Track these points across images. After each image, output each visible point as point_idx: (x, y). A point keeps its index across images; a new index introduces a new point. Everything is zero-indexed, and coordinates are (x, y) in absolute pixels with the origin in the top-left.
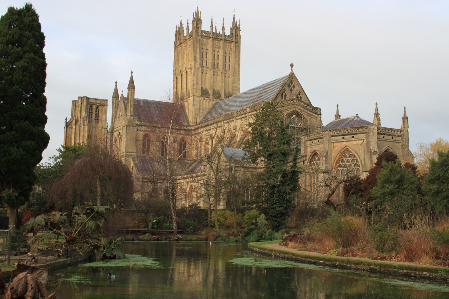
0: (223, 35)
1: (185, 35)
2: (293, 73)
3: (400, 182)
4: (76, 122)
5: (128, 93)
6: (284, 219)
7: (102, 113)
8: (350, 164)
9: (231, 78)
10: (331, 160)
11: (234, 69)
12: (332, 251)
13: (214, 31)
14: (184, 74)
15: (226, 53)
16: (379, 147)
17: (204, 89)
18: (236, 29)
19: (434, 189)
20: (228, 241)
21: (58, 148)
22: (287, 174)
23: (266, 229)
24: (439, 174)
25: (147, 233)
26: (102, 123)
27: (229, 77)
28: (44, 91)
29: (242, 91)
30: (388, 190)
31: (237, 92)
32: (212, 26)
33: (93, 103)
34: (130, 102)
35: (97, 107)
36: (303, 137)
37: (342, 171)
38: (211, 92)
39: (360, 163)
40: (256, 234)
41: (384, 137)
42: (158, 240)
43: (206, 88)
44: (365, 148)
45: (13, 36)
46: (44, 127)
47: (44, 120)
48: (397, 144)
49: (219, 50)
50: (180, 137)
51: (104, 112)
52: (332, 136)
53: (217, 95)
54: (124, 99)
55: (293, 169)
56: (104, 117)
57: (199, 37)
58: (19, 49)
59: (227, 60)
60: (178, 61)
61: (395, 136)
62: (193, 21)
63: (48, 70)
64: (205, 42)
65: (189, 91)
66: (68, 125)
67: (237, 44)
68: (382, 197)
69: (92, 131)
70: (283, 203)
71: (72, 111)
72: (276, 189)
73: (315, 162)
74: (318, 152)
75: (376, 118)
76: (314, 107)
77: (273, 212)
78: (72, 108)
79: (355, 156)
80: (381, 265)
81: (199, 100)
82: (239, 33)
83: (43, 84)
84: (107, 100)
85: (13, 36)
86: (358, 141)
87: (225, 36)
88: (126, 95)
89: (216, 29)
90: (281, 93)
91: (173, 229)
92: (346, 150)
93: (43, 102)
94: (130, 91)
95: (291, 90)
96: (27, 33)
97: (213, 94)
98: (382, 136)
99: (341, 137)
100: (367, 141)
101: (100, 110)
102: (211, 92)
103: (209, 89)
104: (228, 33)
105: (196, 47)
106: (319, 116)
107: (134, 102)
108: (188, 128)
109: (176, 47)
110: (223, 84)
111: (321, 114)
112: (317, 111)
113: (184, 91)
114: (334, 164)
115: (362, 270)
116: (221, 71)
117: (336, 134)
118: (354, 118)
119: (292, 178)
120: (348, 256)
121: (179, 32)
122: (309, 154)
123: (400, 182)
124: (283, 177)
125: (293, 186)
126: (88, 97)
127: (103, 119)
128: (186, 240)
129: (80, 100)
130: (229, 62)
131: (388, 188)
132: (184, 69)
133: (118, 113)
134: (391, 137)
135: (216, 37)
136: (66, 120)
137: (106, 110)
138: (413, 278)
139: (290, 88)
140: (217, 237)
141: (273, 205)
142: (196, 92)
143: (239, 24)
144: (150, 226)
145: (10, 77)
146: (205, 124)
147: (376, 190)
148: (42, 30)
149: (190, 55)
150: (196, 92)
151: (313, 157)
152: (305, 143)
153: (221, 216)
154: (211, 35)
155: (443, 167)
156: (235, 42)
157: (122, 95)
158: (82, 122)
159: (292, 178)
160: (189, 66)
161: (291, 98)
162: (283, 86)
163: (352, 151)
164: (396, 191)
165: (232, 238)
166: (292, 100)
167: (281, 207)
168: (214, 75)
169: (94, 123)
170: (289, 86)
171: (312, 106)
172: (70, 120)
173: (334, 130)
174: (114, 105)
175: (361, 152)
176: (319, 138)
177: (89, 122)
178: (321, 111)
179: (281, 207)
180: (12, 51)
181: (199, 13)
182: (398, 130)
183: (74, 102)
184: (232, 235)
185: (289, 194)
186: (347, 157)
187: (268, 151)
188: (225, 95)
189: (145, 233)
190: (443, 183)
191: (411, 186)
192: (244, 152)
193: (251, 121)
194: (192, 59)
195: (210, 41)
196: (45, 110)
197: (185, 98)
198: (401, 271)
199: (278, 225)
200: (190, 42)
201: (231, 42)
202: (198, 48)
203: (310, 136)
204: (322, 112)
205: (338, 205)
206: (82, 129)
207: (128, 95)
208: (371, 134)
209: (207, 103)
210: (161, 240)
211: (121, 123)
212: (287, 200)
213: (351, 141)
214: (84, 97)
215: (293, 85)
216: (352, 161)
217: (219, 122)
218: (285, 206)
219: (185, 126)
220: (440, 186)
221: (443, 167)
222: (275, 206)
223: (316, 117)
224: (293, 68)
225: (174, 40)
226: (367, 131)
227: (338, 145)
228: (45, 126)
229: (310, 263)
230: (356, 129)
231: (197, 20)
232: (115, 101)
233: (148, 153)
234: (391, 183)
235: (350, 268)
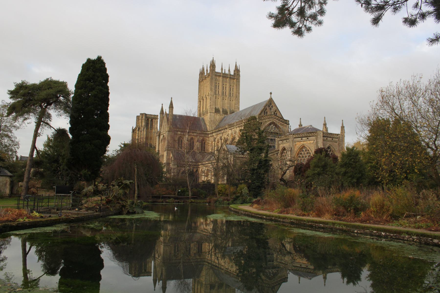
0: (229, 75)
1: (205, 74)
2: (272, 98)
3: (324, 167)
4: (139, 129)
5: (169, 111)
6: (260, 190)
7: (155, 123)
8: (306, 156)
9: (234, 102)
10: (294, 153)
11: (236, 96)
12: (276, 210)
13: (223, 72)
14: (205, 99)
15: (231, 86)
16: (324, 145)
17: (217, 108)
18: (237, 71)
19: (343, 171)
20: (223, 204)
21: (119, 145)
22: (262, 162)
23: (248, 196)
24: (346, 162)
25: (171, 198)
26: (154, 130)
27: (233, 101)
28: (107, 109)
29: (241, 109)
30: (317, 172)
31: (238, 110)
32: (222, 69)
33: (149, 117)
34: (170, 116)
35: (152, 120)
36: (276, 139)
37: (301, 160)
38: (221, 110)
40: (241, 200)
41: (327, 139)
42: (179, 202)
43: (218, 108)
44: (315, 145)
45: (89, 76)
46: (108, 132)
47: (108, 127)
48: (335, 143)
49: (227, 84)
50: (201, 138)
51: (156, 122)
52: (295, 138)
53: (225, 112)
54: (166, 114)
55: (266, 159)
56: (156, 126)
57: (214, 76)
58: (92, 84)
59: (232, 90)
60: (201, 91)
61: (334, 138)
62: (210, 66)
63: (110, 97)
64: (218, 79)
65: (207, 110)
66: (134, 131)
67: (238, 80)
68: (313, 176)
69: (148, 135)
70: (259, 180)
71: (136, 122)
72: (255, 171)
73: (284, 154)
74: (286, 148)
75: (324, 127)
76: (285, 120)
77: (253, 186)
78: (137, 120)
79: (309, 151)
80: (297, 220)
81: (213, 115)
82: (239, 73)
83: (108, 105)
84: (158, 115)
85: (89, 76)
86: (310, 141)
87: (230, 75)
88: (168, 112)
89: (225, 71)
90: (264, 111)
91: (189, 195)
92: (303, 147)
93: (106, 117)
94: (170, 110)
95: (271, 109)
96: (98, 74)
97: (222, 111)
98: (325, 138)
99: (300, 139)
100: (316, 141)
101: (153, 121)
102: (221, 110)
103: (220, 108)
104: (232, 73)
105: (212, 82)
106: (288, 125)
107: (172, 116)
108: (206, 133)
109: (200, 82)
110: (229, 105)
111: (289, 124)
112: (286, 122)
113: (204, 109)
114: (296, 155)
115: (286, 222)
116: (227, 97)
117: (297, 136)
118: (309, 127)
119: (265, 164)
120: (284, 214)
121: (202, 73)
122: (280, 149)
123: (324, 167)
124: (259, 164)
125: (266, 169)
126: (146, 113)
127: (155, 127)
128: (196, 203)
129: (141, 116)
130: (233, 91)
131: (317, 170)
132: (205, 96)
133: (163, 123)
134: (331, 139)
135: (225, 76)
136: (133, 128)
137: (157, 122)
138: (314, 228)
139: (270, 107)
140: (216, 201)
141: (253, 181)
142: (212, 110)
143: (239, 68)
144: (176, 194)
145: (86, 101)
146: (217, 130)
147: (309, 172)
148: (107, 72)
149: (208, 87)
150: (212, 110)
151: (283, 151)
152: (278, 142)
153: (223, 188)
154: (222, 75)
155: (349, 157)
156: (237, 79)
157: (166, 112)
158: (142, 129)
159: (265, 164)
160: (208, 94)
161: (270, 114)
162: (265, 107)
163: (307, 147)
164: (322, 172)
165: (225, 201)
166: (271, 115)
167: (258, 182)
168: (223, 99)
169: (149, 129)
170: (269, 106)
171: (283, 119)
172: (135, 128)
173: (296, 134)
174: (161, 118)
175: (312, 148)
176: (287, 139)
177: (147, 129)
178: (289, 122)
179: (258, 182)
180: (88, 85)
182: (336, 134)
183: (138, 117)
184: (226, 200)
185: (263, 174)
186: (304, 151)
187: (250, 147)
188: (230, 112)
189: (169, 198)
190: (349, 167)
191: (331, 169)
192: (236, 148)
193: (242, 128)
194: (209, 89)
195: (221, 78)
196: (108, 121)
197: (205, 114)
198: (308, 223)
199: (256, 194)
200: (208, 79)
201: (234, 79)
202: (213, 83)
203: (281, 138)
204: (290, 123)
205: (288, 181)
206: (142, 133)
207: (169, 112)
208: (319, 137)
209: (218, 117)
210: (181, 203)
211: (165, 130)
212: (262, 178)
213: (307, 141)
214: (144, 114)
215: (271, 106)
216: (307, 154)
217: (225, 129)
218: (261, 182)
219: (205, 131)
220: (347, 170)
221: (349, 157)
222: (254, 182)
223: (286, 126)
224: (272, 95)
225: (199, 78)
226: (316, 135)
227: (298, 144)
228: (108, 131)
229: (258, 218)
230: (310, 134)
231: (213, 65)
232: (161, 116)
233: (181, 149)
234: (319, 167)
235: (280, 221)
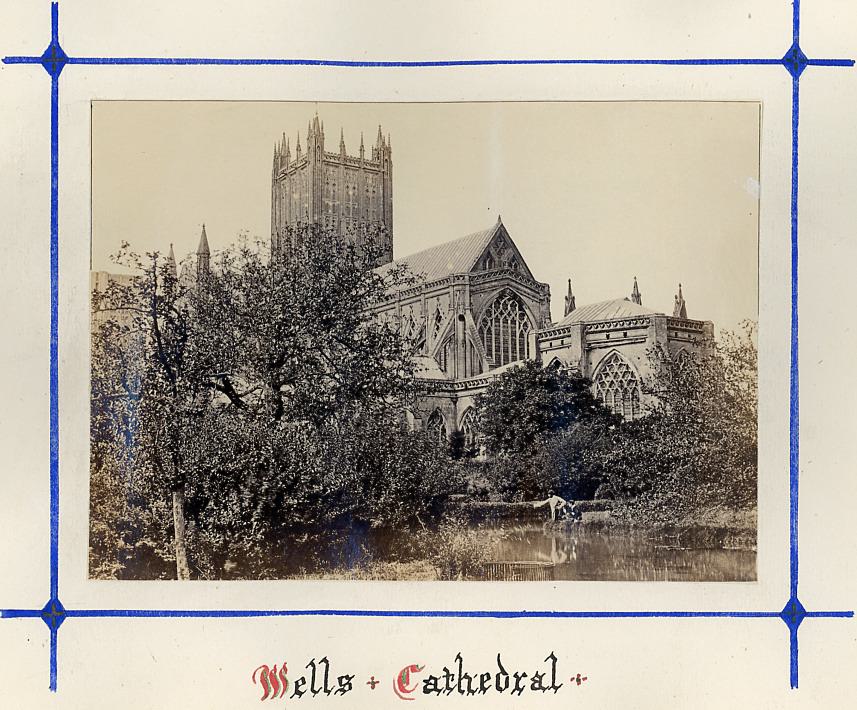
1: (293, 158)
18: (384, 153)
32: (342, 146)
39: (638, 378)
79: (628, 367)
104: (368, 156)
109: (275, 181)
112: (542, 292)
121: (280, 159)
135: (346, 162)
171: (534, 282)
181: (320, 122)
231: (317, 136)
